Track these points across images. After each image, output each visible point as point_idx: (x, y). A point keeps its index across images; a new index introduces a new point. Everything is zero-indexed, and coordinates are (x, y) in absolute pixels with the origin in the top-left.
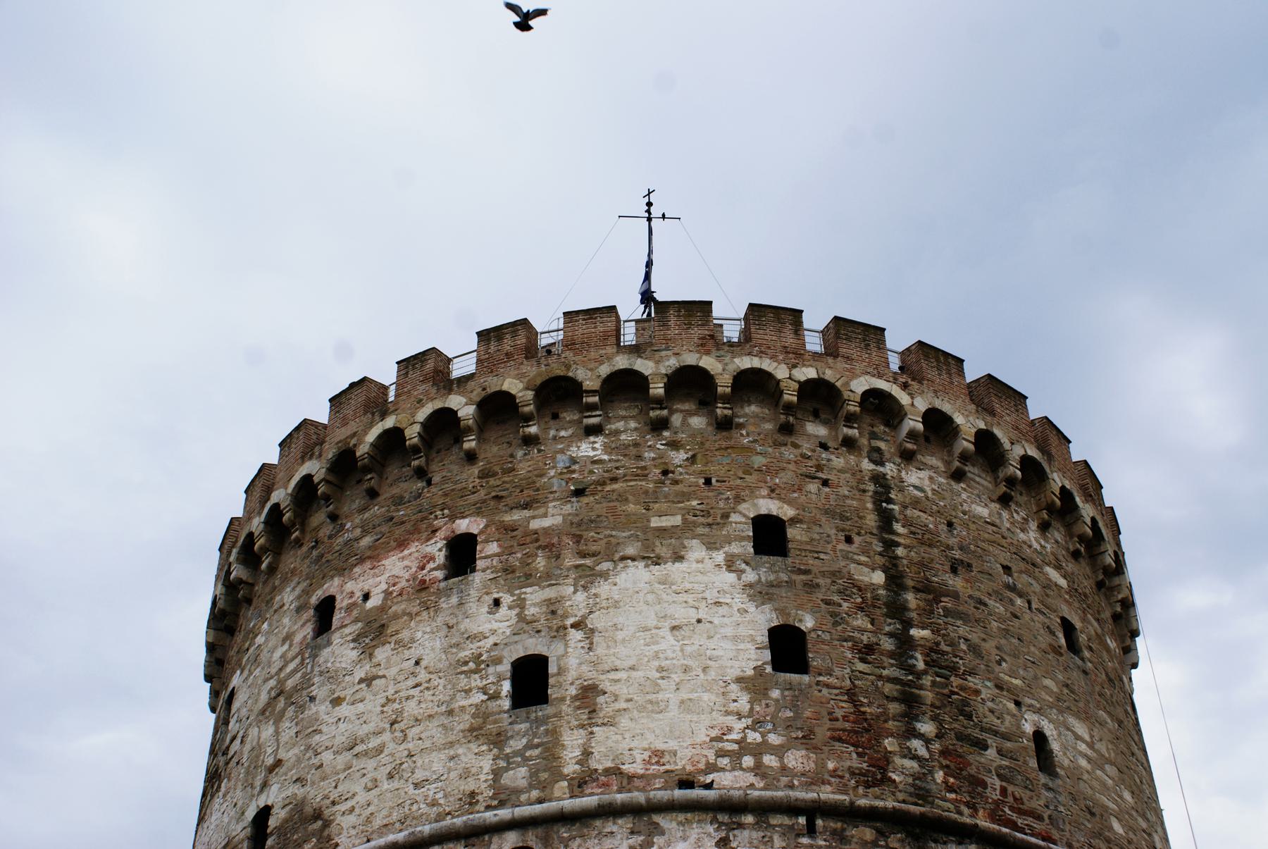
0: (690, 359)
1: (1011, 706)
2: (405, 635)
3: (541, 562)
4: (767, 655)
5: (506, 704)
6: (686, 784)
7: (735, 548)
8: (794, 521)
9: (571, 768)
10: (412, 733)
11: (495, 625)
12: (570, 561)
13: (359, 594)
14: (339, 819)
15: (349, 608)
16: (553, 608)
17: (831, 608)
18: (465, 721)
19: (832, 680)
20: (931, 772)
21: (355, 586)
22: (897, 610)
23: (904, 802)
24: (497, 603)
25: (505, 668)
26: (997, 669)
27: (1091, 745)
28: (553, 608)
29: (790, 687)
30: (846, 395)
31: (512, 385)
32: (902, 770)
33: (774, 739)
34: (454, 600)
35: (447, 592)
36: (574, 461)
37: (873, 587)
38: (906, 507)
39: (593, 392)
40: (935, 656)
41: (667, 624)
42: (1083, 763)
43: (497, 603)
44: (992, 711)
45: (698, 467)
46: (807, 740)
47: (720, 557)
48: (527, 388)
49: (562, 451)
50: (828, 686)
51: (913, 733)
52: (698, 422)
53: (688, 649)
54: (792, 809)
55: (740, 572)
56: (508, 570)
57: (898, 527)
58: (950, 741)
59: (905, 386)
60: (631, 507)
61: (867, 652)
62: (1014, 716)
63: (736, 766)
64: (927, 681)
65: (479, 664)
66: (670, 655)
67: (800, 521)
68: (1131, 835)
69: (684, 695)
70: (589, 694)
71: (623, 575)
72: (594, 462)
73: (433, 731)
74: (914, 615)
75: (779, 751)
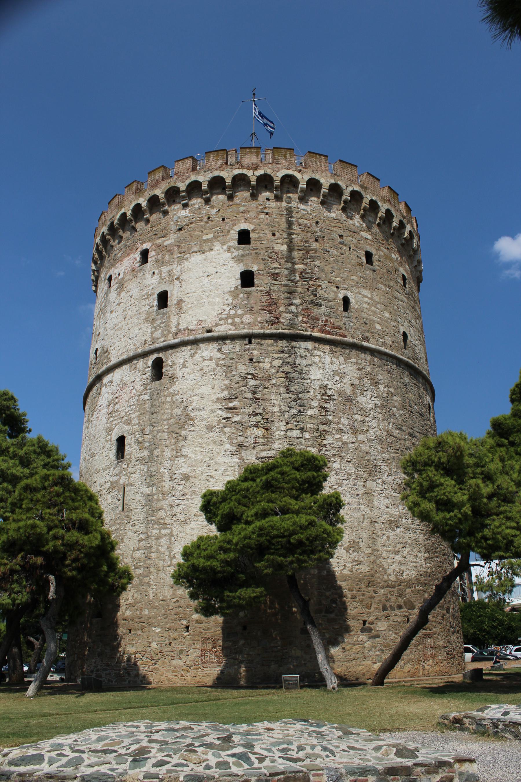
0: (216, 173)
2: (128, 287)
3: (167, 257)
4: (239, 282)
5: (155, 308)
6: (209, 331)
7: (231, 244)
8: (253, 230)
10: (129, 321)
11: (153, 281)
12: (176, 255)
14: (112, 352)
16: (170, 273)
17: (264, 262)
18: (144, 316)
19: (262, 288)
20: (297, 317)
21: (116, 271)
22: (290, 259)
23: (285, 329)
24: (154, 273)
25: (155, 296)
26: (330, 275)
27: (371, 299)
28: (170, 273)
29: (247, 293)
32: (285, 318)
33: (239, 312)
34: (142, 273)
36: (179, 218)
37: (282, 251)
38: (298, 219)
39: (183, 191)
40: (303, 274)
41: (206, 275)
42: (365, 306)
43: (154, 273)
44: (325, 292)
45: (220, 214)
46: (251, 311)
47: (225, 247)
49: (175, 215)
50: (260, 291)
52: (222, 197)
53: (212, 283)
54: (242, 337)
57: (295, 227)
58: (307, 304)
59: (300, 171)
60: (197, 233)
61: (275, 276)
62: (335, 292)
63: (226, 323)
64: (299, 284)
66: (206, 285)
67: (256, 230)
68: (385, 329)
69: (210, 300)
70: (180, 302)
71: (193, 259)
72: (185, 217)
73: (136, 321)
75: (241, 316)
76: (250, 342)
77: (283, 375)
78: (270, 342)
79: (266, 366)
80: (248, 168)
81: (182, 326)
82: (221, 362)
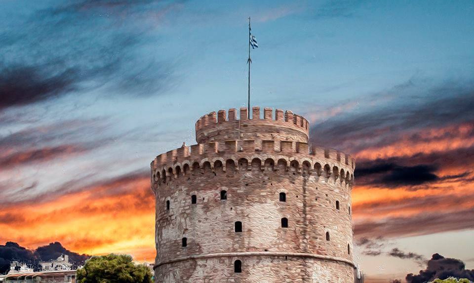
1: (323, 228)
5: (234, 231)
6: (266, 250)
9: (246, 246)
13: (202, 198)
15: (200, 200)
22: (304, 212)
30: (300, 163)
31: (233, 158)
32: (302, 246)
33: (281, 241)
34: (222, 206)
35: (220, 204)
36: (246, 177)
43: (231, 208)
46: (286, 241)
48: (236, 160)
51: (305, 238)
52: (270, 169)
54: (283, 256)
55: (277, 206)
56: (233, 201)
57: (306, 192)
59: (312, 158)
61: (298, 222)
65: (229, 222)
70: (250, 230)
71: (255, 207)
74: (307, 212)
75: (282, 244)
76: (286, 258)
77: (301, 277)
78: (295, 259)
79: (293, 272)
80: (287, 155)
81: (252, 246)
82: (273, 268)
